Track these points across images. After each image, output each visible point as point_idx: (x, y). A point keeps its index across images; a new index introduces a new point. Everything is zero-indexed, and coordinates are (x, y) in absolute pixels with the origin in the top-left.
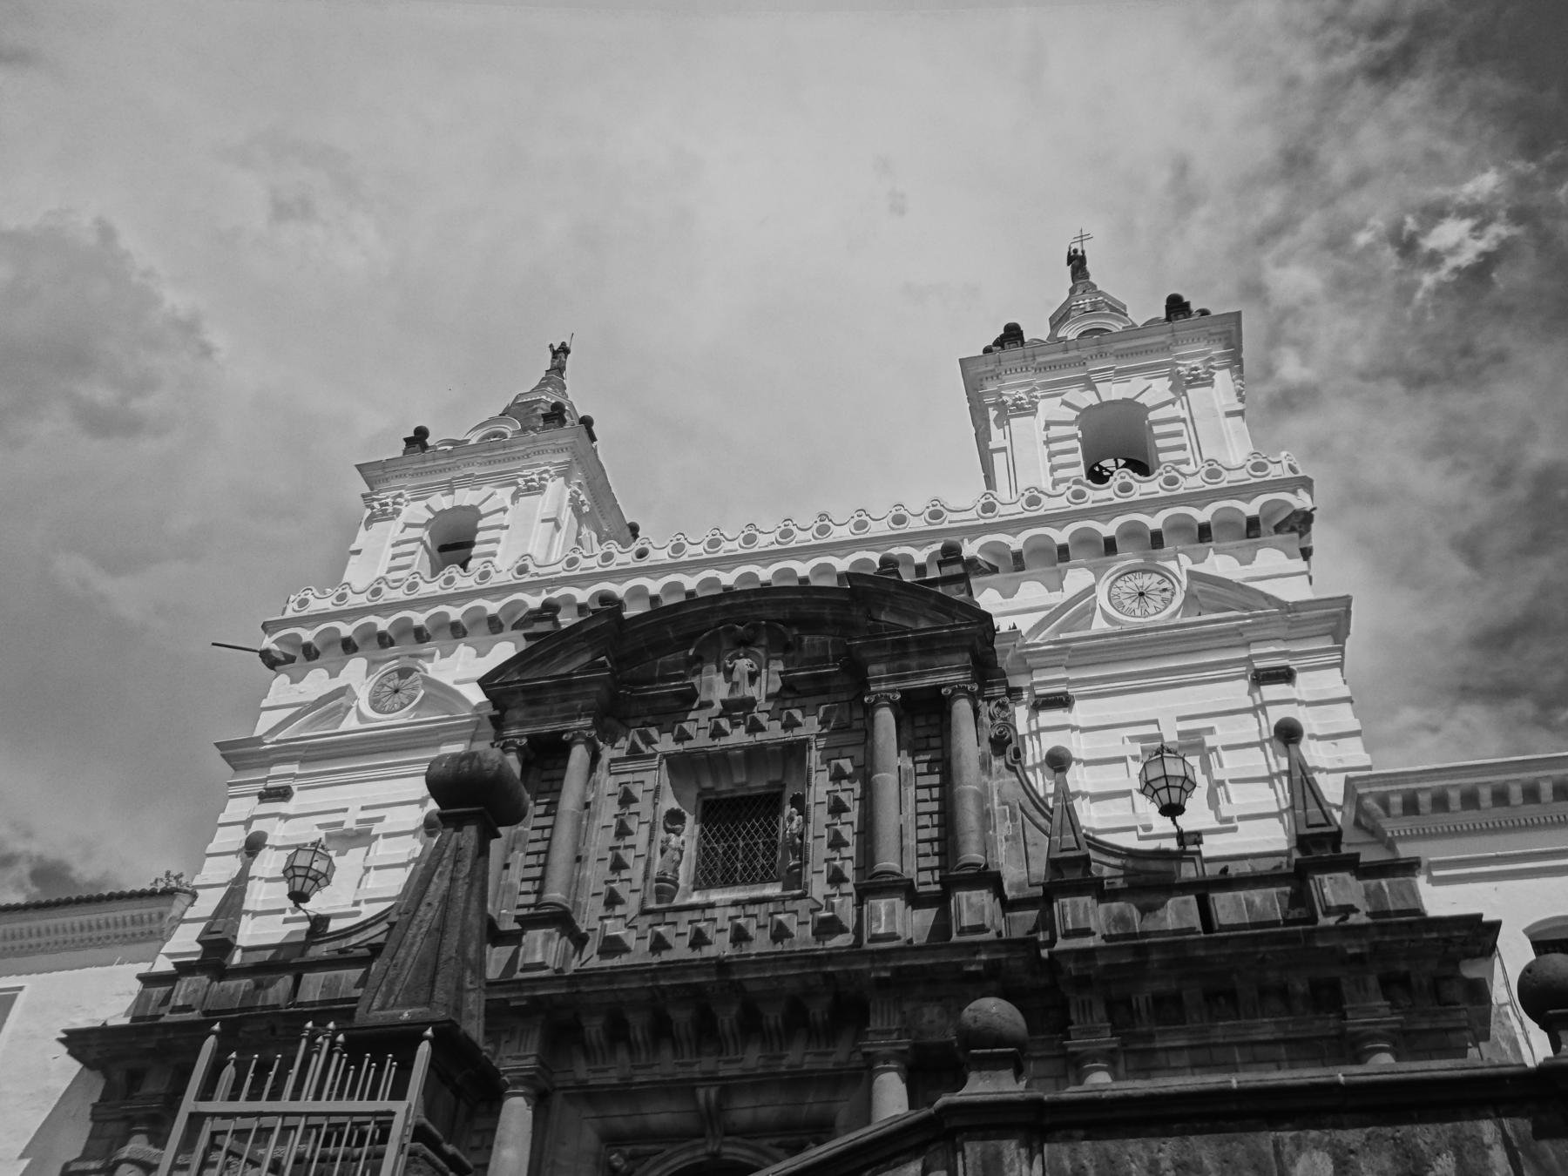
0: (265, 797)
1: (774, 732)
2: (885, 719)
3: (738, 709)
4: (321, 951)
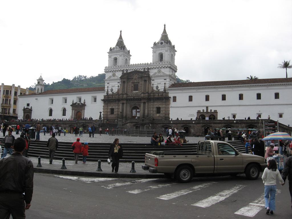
0: (108, 83)
1: (137, 81)
2: (143, 81)
3: (135, 79)
4: (114, 94)
